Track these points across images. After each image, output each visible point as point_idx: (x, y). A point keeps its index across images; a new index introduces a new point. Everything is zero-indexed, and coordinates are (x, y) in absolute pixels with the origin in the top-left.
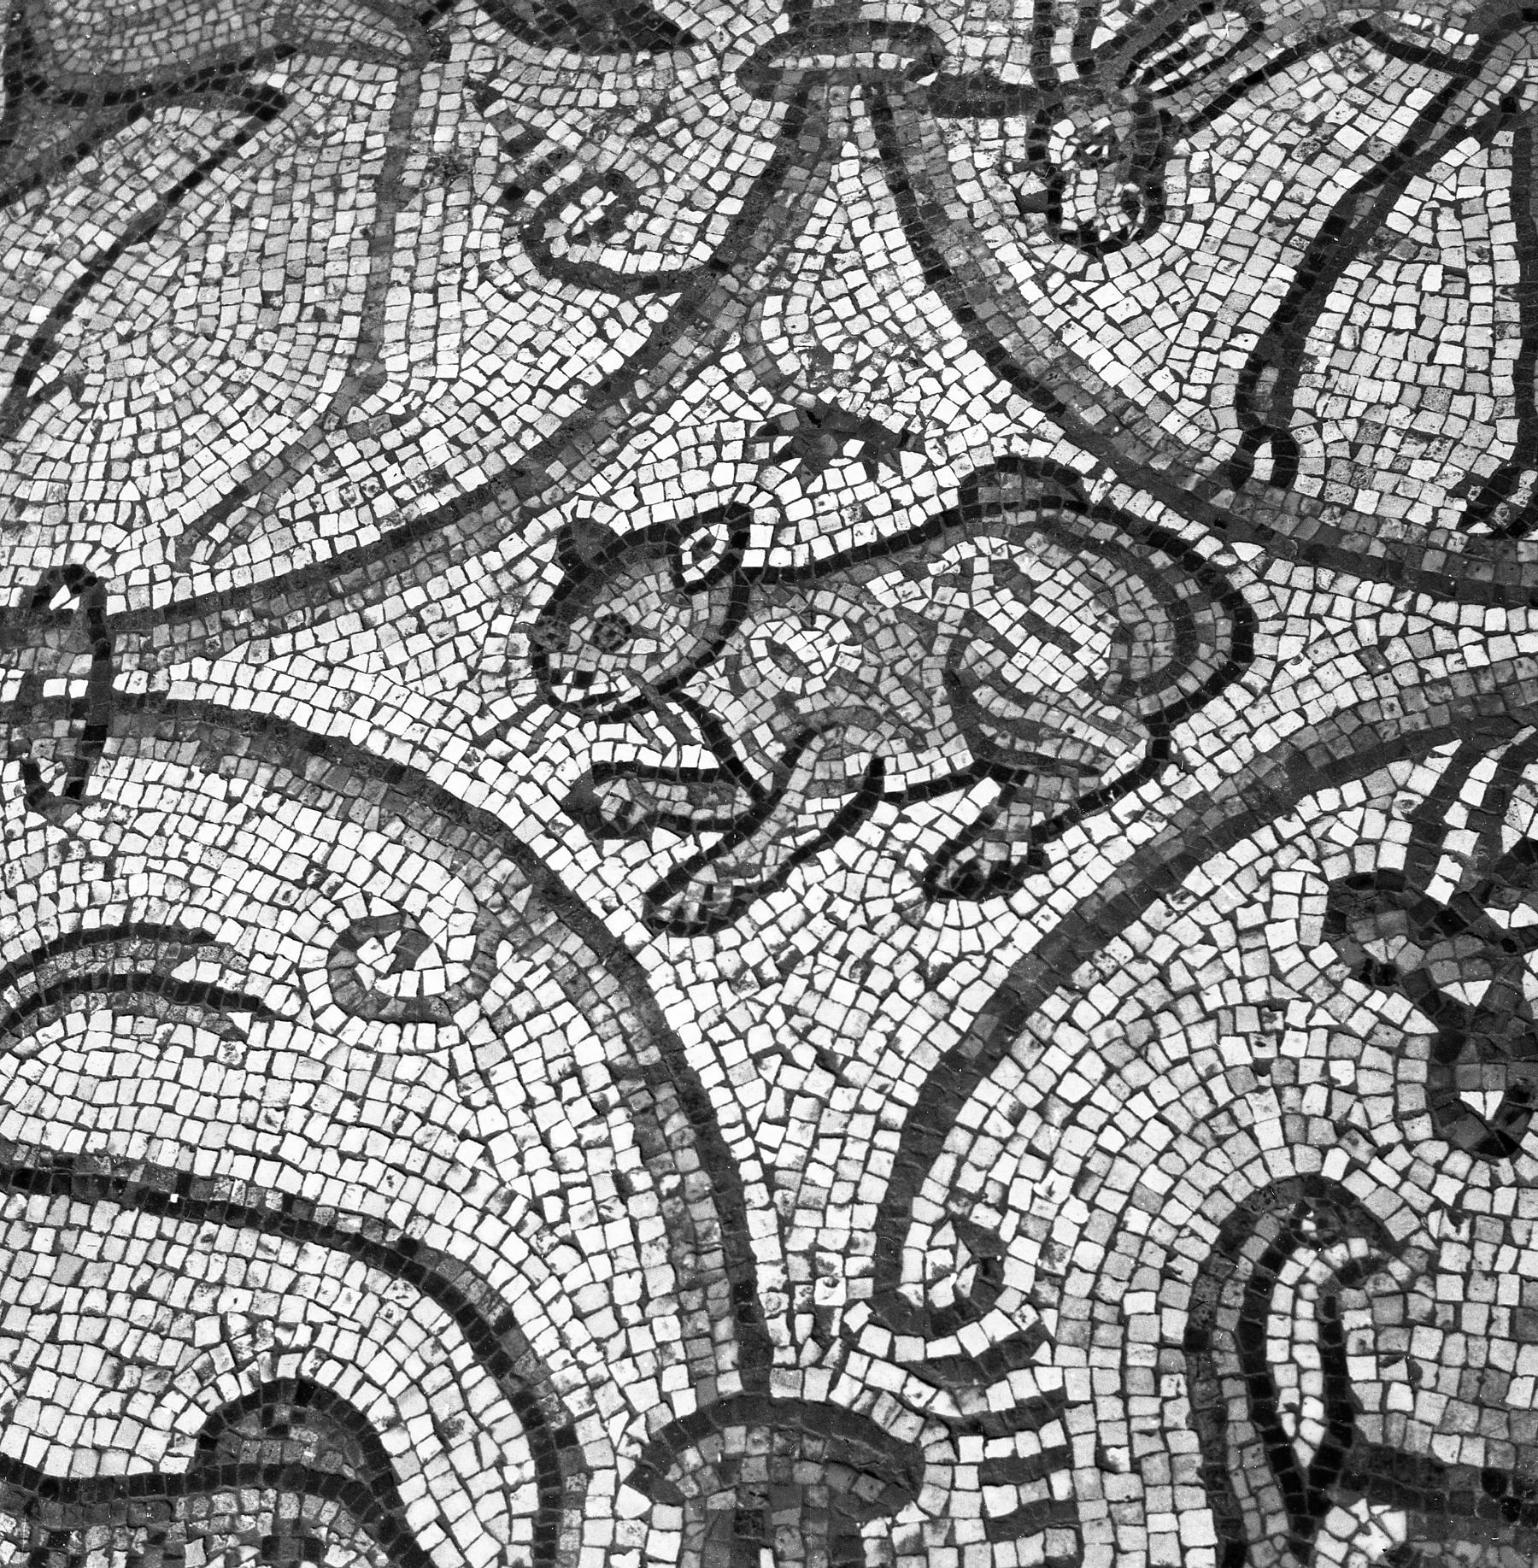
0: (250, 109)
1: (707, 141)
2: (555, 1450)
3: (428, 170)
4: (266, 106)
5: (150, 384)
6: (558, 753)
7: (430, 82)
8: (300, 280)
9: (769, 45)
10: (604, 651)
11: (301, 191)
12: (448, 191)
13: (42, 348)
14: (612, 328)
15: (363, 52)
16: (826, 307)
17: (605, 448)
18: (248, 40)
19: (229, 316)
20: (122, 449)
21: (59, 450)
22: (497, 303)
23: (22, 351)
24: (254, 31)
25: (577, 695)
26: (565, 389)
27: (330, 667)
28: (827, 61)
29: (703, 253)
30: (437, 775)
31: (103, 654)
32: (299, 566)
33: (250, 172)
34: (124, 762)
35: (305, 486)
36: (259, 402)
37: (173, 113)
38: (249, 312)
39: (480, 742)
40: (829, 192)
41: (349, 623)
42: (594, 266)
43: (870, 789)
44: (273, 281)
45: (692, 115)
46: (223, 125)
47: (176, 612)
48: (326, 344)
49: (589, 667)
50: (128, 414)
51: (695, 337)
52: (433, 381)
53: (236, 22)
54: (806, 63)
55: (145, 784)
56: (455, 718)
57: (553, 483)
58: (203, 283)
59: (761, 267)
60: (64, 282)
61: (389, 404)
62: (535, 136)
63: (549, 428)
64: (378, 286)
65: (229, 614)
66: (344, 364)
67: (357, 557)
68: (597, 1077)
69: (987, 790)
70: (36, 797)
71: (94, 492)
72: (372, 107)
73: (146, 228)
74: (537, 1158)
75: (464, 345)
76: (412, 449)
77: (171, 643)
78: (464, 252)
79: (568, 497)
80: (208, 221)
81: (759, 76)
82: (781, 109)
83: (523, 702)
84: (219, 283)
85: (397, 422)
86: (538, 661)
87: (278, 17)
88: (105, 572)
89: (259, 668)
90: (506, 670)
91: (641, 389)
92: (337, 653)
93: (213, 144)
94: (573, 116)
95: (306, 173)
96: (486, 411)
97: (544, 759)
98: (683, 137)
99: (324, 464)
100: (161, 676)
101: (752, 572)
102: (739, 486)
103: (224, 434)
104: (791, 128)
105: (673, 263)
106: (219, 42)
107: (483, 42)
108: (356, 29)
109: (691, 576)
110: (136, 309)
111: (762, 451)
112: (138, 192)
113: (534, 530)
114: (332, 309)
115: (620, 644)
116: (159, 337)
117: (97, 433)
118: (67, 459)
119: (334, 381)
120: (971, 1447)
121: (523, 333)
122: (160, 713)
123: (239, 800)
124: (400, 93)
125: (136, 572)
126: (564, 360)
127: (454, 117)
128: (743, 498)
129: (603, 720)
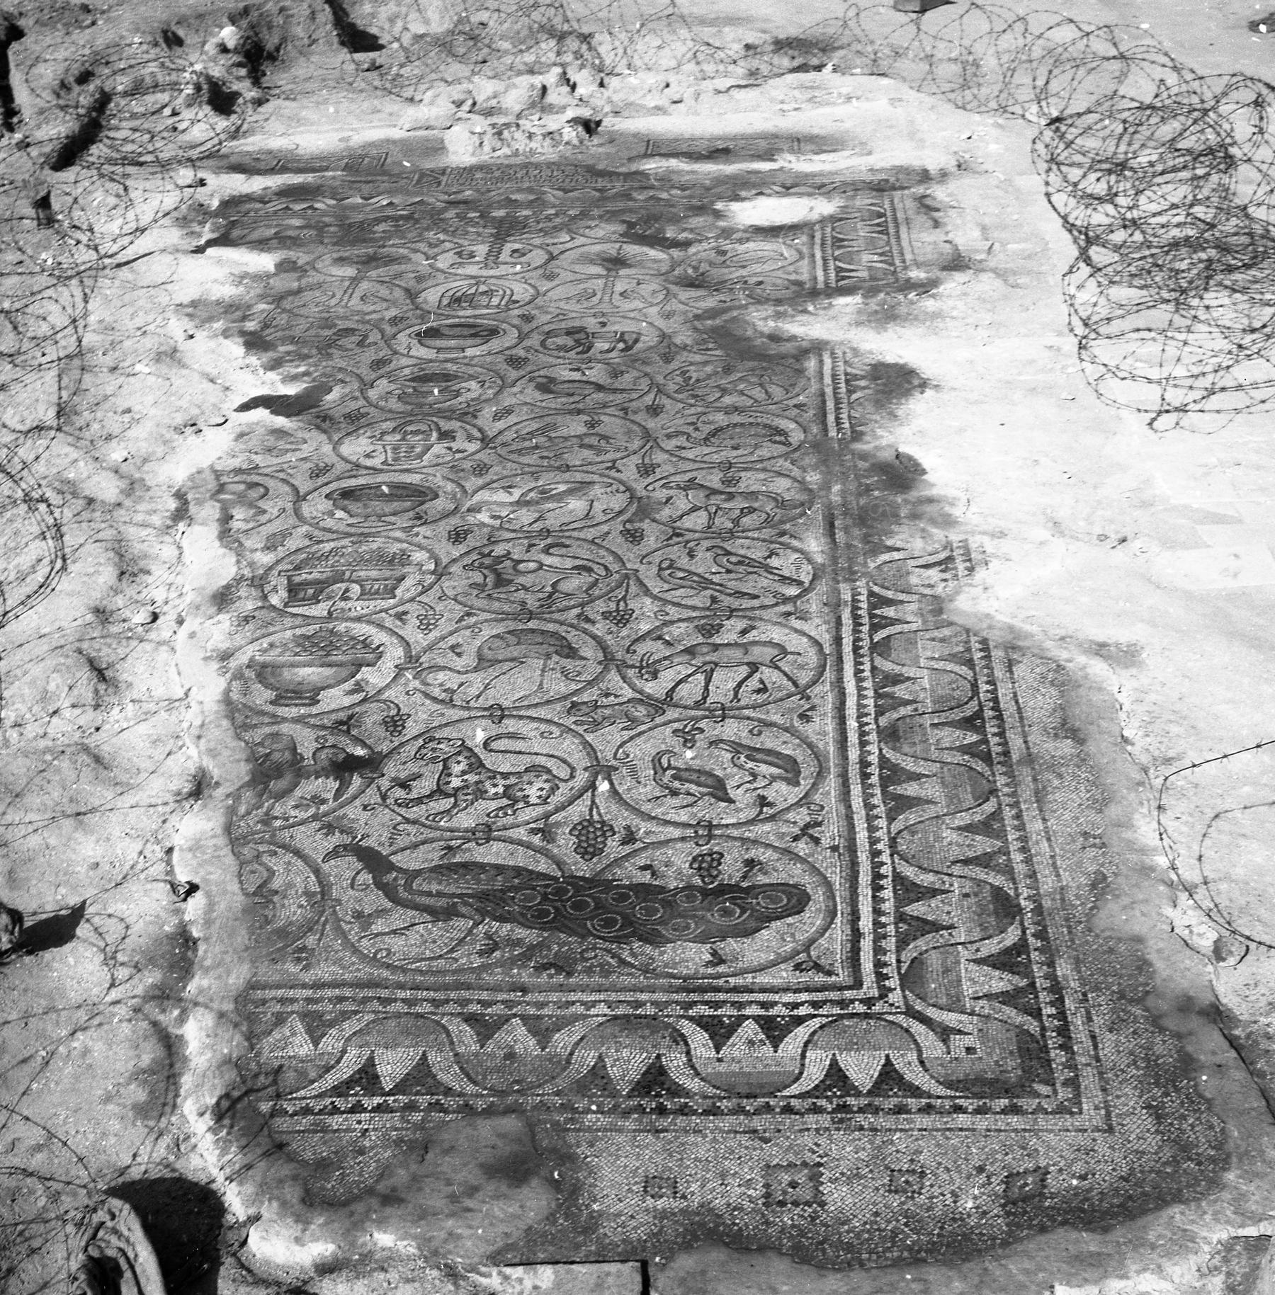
125: (506, 704)
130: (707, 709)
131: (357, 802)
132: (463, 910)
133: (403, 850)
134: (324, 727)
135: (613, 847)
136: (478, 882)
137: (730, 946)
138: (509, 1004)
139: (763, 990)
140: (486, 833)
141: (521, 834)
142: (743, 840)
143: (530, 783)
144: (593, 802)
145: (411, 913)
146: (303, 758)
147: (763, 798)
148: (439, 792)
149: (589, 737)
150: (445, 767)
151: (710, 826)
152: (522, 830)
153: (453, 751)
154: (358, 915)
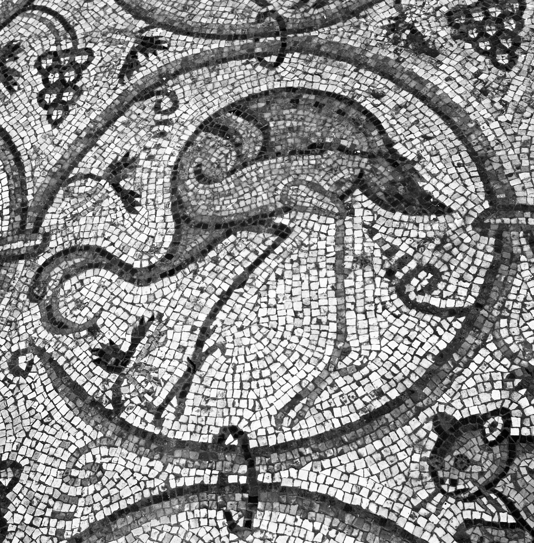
0: (276, 233)
1: (465, 253)
3: (354, 262)
4: (283, 232)
5: (253, 349)
6: (449, 515)
7: (348, 224)
8: (309, 306)
9: (482, 214)
10: (460, 470)
11: (303, 269)
12: (364, 271)
13: (206, 332)
14: (439, 330)
15: (318, 210)
16: (525, 325)
17: (446, 381)
18: (271, 204)
19: (282, 321)
20: (246, 376)
21: (220, 376)
22: (391, 319)
23: (198, 332)
24: (273, 201)
25: (452, 489)
26: (425, 356)
27: (348, 474)
28: (507, 220)
29: (471, 300)
30: (401, 523)
31: (251, 465)
32: (328, 430)
33: (281, 260)
34: (267, 513)
35: (325, 395)
36: (300, 358)
37: (245, 233)
38: (290, 320)
39: (416, 509)
40: (518, 276)
41: (353, 455)
42: (428, 304)
44: (298, 307)
45: (457, 242)
46: (266, 239)
47: (278, 448)
48: (324, 334)
49: (456, 477)
50: (246, 361)
51: (474, 336)
52: (371, 351)
53: (265, 196)
54: (498, 221)
55: (278, 523)
56: (403, 498)
57: (426, 396)
58: (269, 307)
59: (496, 306)
60: (211, 304)
61: (354, 361)
62: (394, 249)
63: (421, 373)
64: (341, 310)
65: (302, 450)
66: (332, 343)
67: (351, 427)
70: (232, 527)
71: (237, 394)
72: (327, 234)
73: (240, 282)
75: (381, 337)
76: (366, 381)
77: (279, 461)
78: (375, 297)
79: (434, 403)
80: (267, 280)
81: (481, 226)
82: (492, 241)
83: (431, 491)
84: (275, 307)
85: (359, 368)
86: (434, 474)
87: (282, 195)
88: (246, 429)
89: (318, 474)
90: (421, 478)
91: (456, 357)
92: (350, 468)
93: (264, 248)
94: (408, 241)
95: (304, 261)
96: (394, 365)
97: (443, 517)
98: (455, 251)
99: (332, 386)
100: (277, 475)
101: (515, 437)
102: (504, 400)
103: (287, 372)
104: (498, 248)
105: (460, 304)
106: (259, 205)
107: (367, 208)
108: (315, 201)
109: (490, 438)
110: (242, 317)
111: (509, 384)
112: (236, 267)
113: (422, 417)
114: (324, 320)
115: (466, 468)
116: (255, 329)
117: (234, 369)
118: (224, 380)
119: (330, 350)
121: (404, 332)
122: (281, 493)
123: (318, 532)
124: (337, 229)
125: (260, 430)
126: (422, 344)
127: (361, 240)
128: (506, 405)
129: (465, 501)
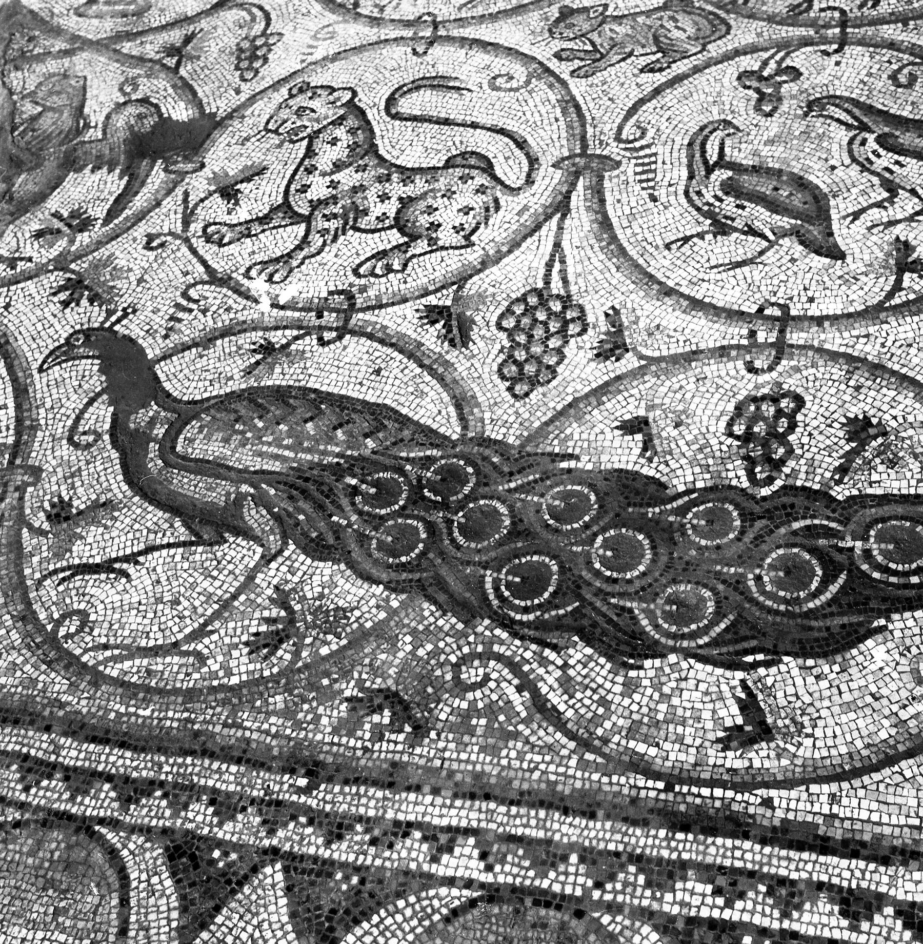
2: (533, 162)
43: (630, 54)
68: (554, 101)
69: (660, 55)
74: (536, 115)
120: (633, 161)
130: (813, 24)
131: (140, 231)
132: (254, 516)
133: (186, 348)
134: (141, 60)
135: (580, 368)
136: (297, 447)
137: (789, 681)
138: (275, 812)
139: (851, 848)
140: (341, 316)
141: (403, 320)
142: (853, 362)
143: (449, 194)
144: (557, 245)
145: (156, 516)
146: (87, 126)
147: (905, 247)
148: (285, 209)
149: (578, 87)
150: (310, 152)
151: (785, 320)
152: (408, 309)
153: (332, 114)
154: (61, 513)
